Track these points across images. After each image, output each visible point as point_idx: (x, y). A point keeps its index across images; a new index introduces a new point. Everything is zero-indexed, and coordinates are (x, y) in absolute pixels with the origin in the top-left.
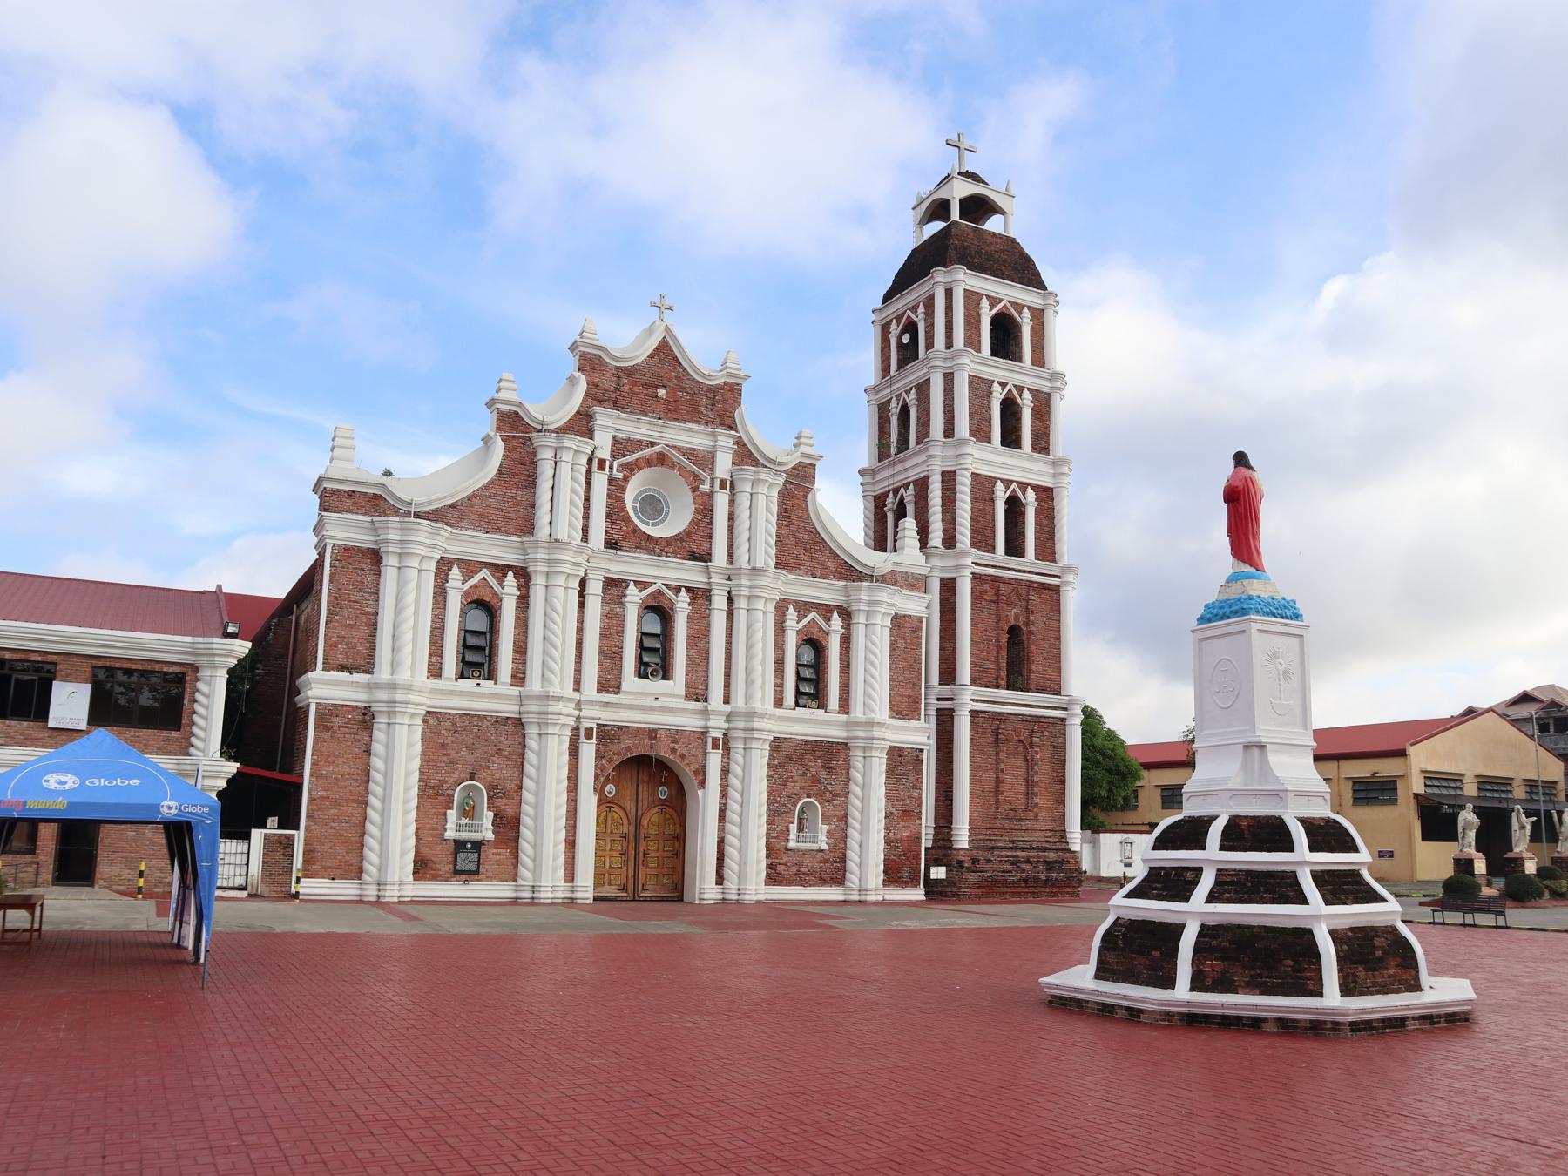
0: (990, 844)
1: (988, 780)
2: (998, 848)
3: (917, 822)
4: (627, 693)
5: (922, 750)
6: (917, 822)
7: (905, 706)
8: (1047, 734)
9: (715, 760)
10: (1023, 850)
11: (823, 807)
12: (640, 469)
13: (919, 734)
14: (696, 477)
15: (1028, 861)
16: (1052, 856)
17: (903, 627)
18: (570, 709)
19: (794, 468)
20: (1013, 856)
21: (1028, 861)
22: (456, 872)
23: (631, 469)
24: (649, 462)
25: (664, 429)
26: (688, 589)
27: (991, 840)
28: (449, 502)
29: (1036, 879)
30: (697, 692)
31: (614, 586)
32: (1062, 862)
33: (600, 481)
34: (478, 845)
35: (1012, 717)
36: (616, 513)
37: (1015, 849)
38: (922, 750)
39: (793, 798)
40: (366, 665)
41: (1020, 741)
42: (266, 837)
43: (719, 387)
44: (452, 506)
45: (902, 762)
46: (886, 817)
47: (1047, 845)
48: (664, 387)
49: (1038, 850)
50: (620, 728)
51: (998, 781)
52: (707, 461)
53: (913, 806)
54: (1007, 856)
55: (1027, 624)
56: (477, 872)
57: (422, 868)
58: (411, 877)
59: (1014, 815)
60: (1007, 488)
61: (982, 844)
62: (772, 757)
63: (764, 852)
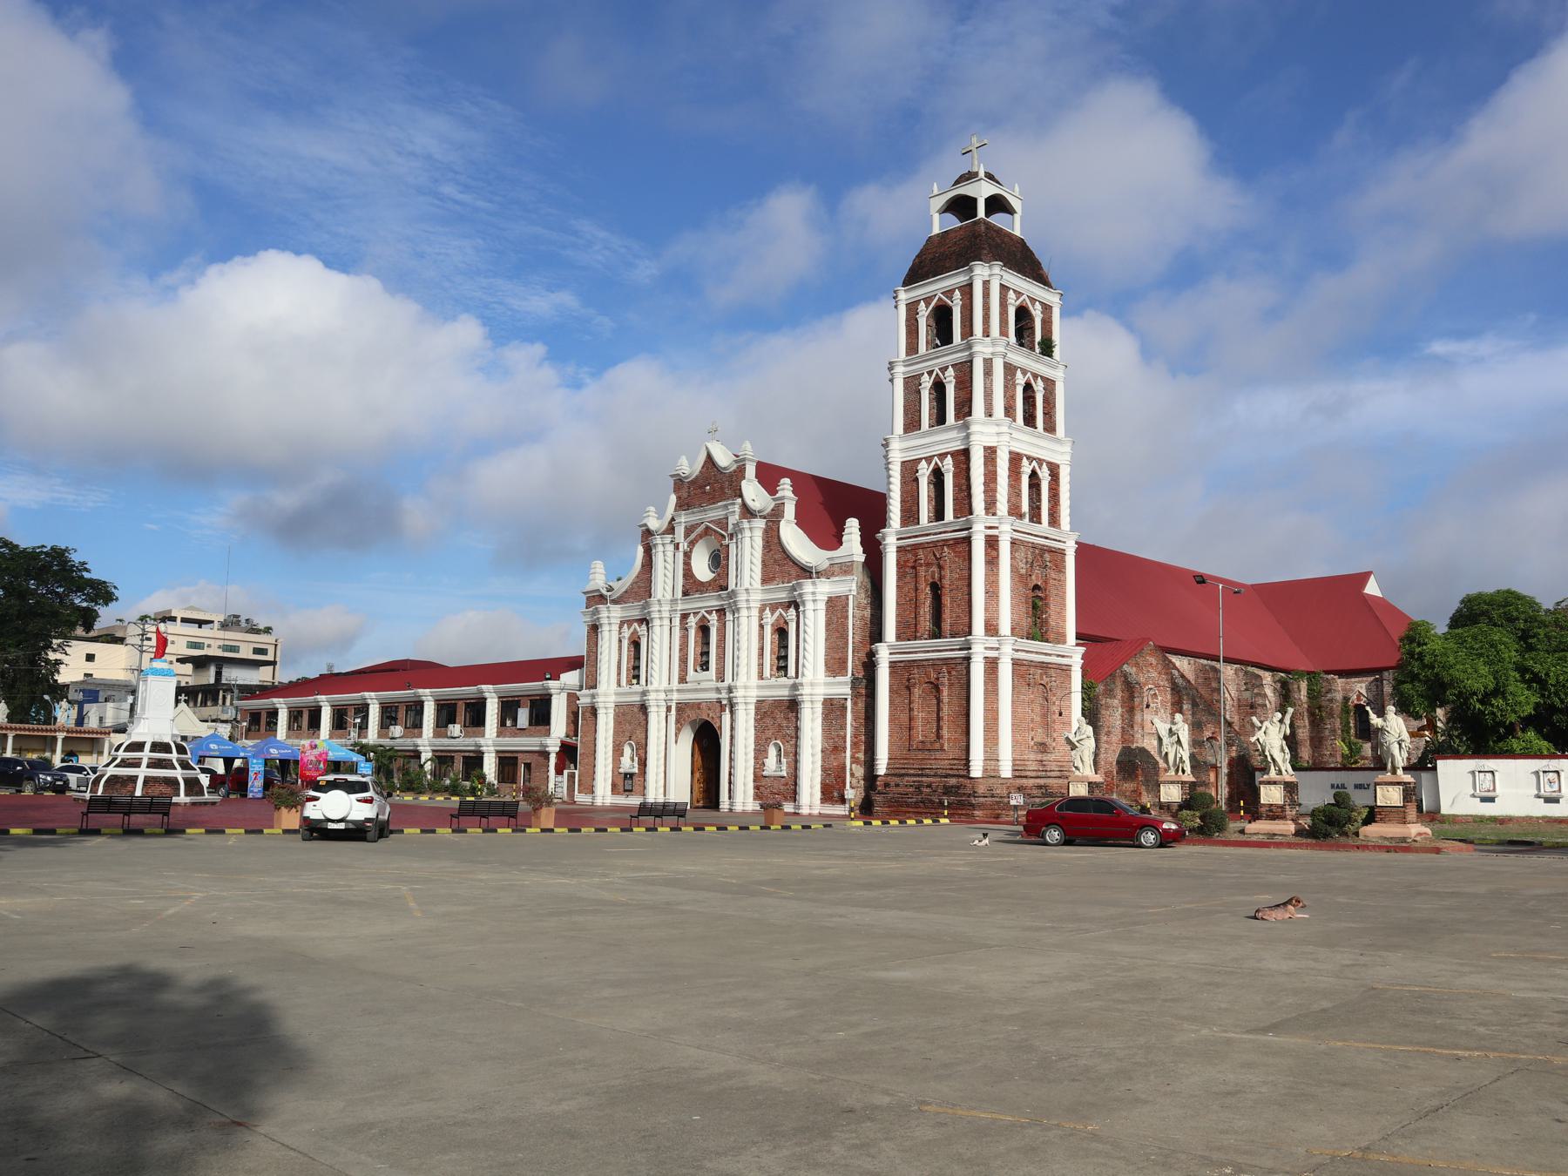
0: (903, 771)
1: (904, 717)
2: (908, 775)
3: (843, 755)
4: (691, 682)
5: (846, 699)
6: (843, 755)
7: (835, 666)
8: (954, 673)
9: (726, 717)
10: (927, 776)
11: (784, 746)
12: (697, 542)
13: (842, 687)
14: (723, 536)
15: (929, 786)
16: (953, 781)
17: (835, 606)
18: (662, 696)
19: (773, 510)
20: (919, 782)
21: (929, 786)
22: (625, 791)
23: (692, 544)
24: (700, 536)
25: (707, 513)
26: (717, 611)
27: (904, 768)
28: (624, 590)
29: (931, 801)
30: (721, 676)
31: (685, 617)
32: (958, 787)
33: (680, 556)
34: (632, 775)
35: (924, 663)
36: (688, 573)
37: (922, 775)
38: (846, 699)
39: (768, 740)
40: (595, 687)
41: (932, 683)
42: (568, 773)
43: (735, 471)
44: (626, 592)
45: (833, 709)
46: (822, 751)
47: (951, 772)
48: (709, 484)
49: (941, 776)
50: (686, 704)
51: (911, 719)
52: (723, 523)
53: (840, 743)
54: (914, 782)
55: (940, 579)
56: (631, 791)
57: (615, 789)
58: (610, 793)
59: (924, 748)
60: (929, 464)
61: (897, 771)
62: (756, 714)
63: (751, 777)
